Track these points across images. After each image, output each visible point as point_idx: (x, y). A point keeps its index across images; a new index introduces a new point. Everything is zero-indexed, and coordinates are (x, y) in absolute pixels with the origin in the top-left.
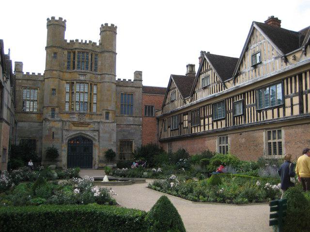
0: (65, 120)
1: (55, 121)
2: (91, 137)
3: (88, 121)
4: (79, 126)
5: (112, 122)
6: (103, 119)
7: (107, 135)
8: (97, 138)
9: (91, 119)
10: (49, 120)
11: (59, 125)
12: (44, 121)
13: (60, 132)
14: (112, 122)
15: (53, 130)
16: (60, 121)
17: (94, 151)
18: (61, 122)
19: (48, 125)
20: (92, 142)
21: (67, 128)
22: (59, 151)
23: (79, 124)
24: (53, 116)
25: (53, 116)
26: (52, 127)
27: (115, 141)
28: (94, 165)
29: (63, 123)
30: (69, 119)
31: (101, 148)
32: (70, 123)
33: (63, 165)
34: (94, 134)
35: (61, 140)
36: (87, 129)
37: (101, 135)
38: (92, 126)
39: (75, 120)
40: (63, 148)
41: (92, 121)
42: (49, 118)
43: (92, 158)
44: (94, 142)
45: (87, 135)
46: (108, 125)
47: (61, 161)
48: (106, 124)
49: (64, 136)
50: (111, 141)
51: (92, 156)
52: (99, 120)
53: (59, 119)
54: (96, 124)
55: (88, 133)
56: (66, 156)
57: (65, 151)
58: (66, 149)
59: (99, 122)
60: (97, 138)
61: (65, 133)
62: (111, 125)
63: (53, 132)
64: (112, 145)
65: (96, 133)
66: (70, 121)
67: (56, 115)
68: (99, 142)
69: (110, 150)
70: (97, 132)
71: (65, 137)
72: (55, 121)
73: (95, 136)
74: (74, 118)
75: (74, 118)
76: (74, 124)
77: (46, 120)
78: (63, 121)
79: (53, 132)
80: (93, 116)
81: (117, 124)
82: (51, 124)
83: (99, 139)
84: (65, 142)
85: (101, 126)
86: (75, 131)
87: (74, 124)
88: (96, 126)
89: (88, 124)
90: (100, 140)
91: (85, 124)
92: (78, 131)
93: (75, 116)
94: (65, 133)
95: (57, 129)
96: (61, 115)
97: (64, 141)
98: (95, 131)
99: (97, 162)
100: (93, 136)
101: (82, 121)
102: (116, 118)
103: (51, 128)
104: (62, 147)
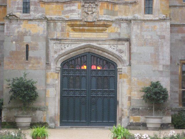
0: (54, 17)
1: (30, 20)
2: (113, 55)
3: (104, 17)
4: (83, 31)
5: (160, 20)
6: (139, 11)
7: (148, 50)
8: (125, 57)
9: (113, 13)
10: (17, 19)
11: (40, 28)
12: (6, 22)
13: (41, 45)
14: (160, 20)
15: (27, 40)
16: (40, 20)
17: (119, 85)
18: (44, 24)
19: (17, 28)
20: (115, 65)
21: (57, 34)
22: (39, 88)
23: (84, 25)
24: (26, 9)
25: (26, 9)
26: (25, 34)
27: (168, 63)
28: (121, 119)
29: (48, 25)
30: (63, 16)
31: (134, 79)
32: (64, 24)
33: (51, 118)
34: (120, 47)
35: (43, 61)
36: (102, 36)
37: (134, 49)
38: (114, 30)
39: (75, 16)
40: (50, 81)
41: (114, 18)
42: (19, 14)
43: (116, 103)
44: (120, 66)
45: (104, 50)
46: (151, 24)
47: (44, 109)
48: (145, 25)
49: (52, 54)
50: (157, 62)
51: (115, 97)
52: (130, 17)
53: (38, 15)
54: (124, 25)
55: (106, 47)
56: (58, 98)
57: (54, 86)
58: (58, 82)
59: (130, 21)
60: (125, 57)
61: (53, 46)
62: (158, 25)
63: (27, 46)
64: (161, 72)
65: (124, 46)
66: (63, 20)
67: (32, 8)
68: (130, 65)
69: (156, 85)
70: (126, 44)
71: (53, 56)
72: (30, 20)
73: (121, 51)
74: (73, 11)
75: (73, 11)
76: (74, 25)
77: (11, 18)
78: (48, 21)
79: (27, 46)
80: (117, 7)
81: (171, 25)
82: (23, 27)
83: (130, 59)
84: (55, 66)
85: (135, 29)
86: (75, 42)
87: (74, 25)
88: (122, 31)
89: (106, 25)
90: (133, 62)
91: (99, 26)
92: (84, 41)
93: (73, 8)
94: (53, 46)
95: (36, 37)
96: (46, 7)
97: (53, 65)
98: (119, 40)
99: (126, 112)
100: (117, 53)
101: (90, 19)
102: (172, 10)
103: (22, 35)
104: (46, 77)
